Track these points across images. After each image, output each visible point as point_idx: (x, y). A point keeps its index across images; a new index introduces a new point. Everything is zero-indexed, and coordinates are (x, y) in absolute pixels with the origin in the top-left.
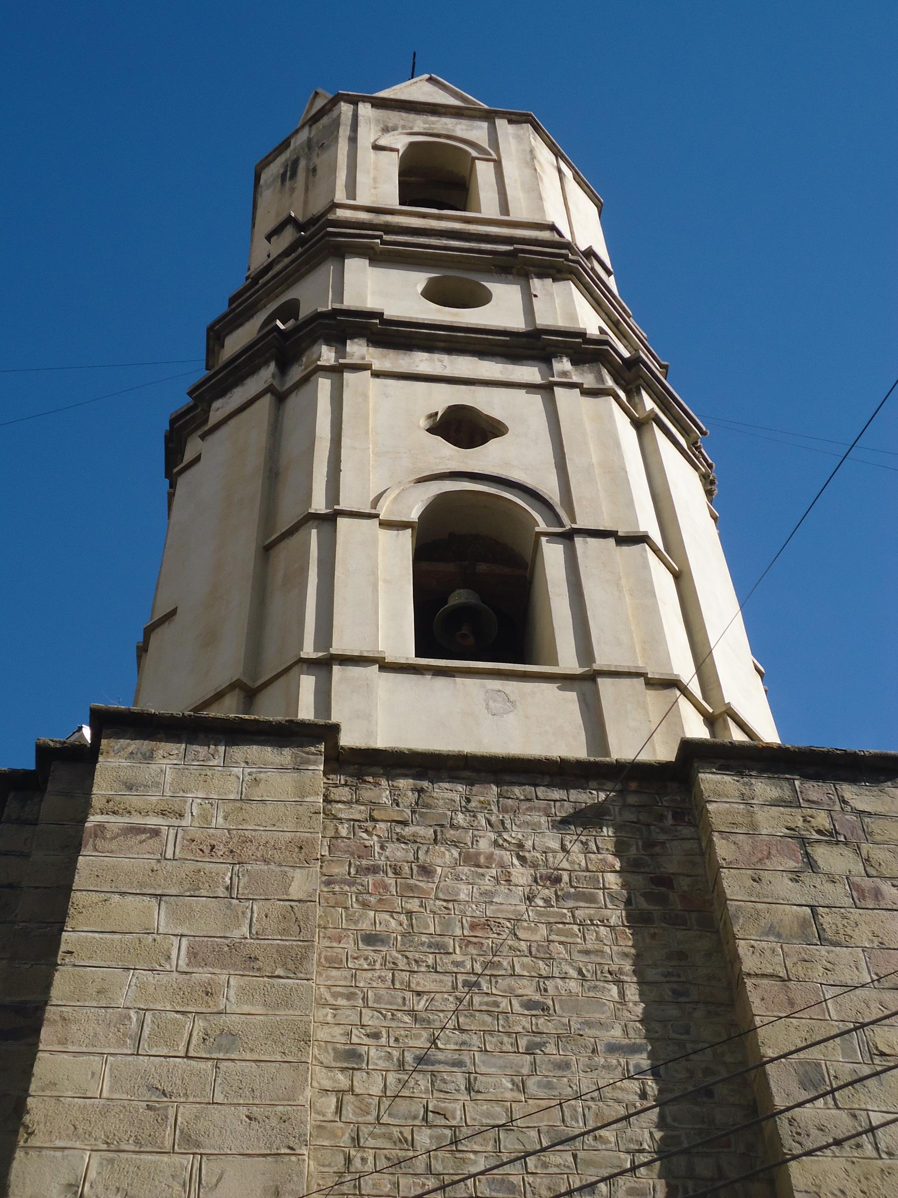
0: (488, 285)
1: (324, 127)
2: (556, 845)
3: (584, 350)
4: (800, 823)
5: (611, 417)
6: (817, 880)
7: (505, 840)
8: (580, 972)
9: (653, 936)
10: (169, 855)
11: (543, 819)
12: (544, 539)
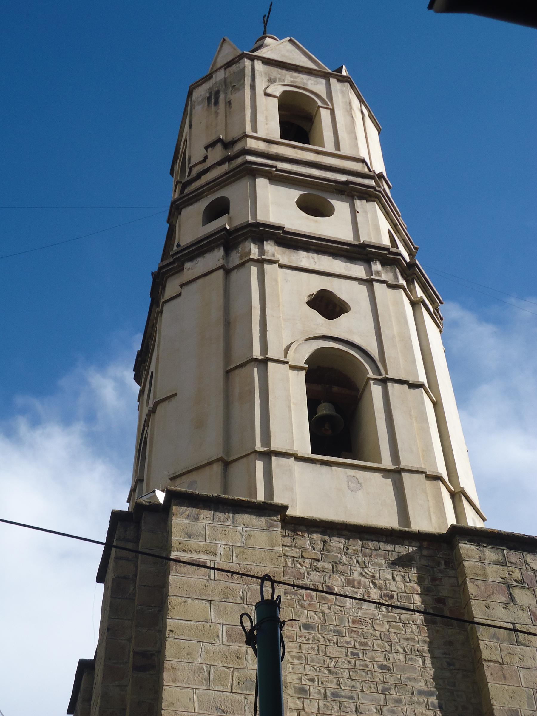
0: (332, 201)
1: (234, 73)
2: (390, 577)
3: (388, 258)
4: (507, 576)
5: (402, 303)
6: (516, 609)
7: (366, 573)
8: (404, 650)
9: (437, 631)
10: (212, 577)
11: (384, 562)
12: (372, 382)
